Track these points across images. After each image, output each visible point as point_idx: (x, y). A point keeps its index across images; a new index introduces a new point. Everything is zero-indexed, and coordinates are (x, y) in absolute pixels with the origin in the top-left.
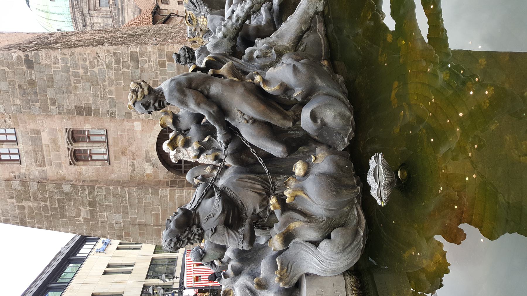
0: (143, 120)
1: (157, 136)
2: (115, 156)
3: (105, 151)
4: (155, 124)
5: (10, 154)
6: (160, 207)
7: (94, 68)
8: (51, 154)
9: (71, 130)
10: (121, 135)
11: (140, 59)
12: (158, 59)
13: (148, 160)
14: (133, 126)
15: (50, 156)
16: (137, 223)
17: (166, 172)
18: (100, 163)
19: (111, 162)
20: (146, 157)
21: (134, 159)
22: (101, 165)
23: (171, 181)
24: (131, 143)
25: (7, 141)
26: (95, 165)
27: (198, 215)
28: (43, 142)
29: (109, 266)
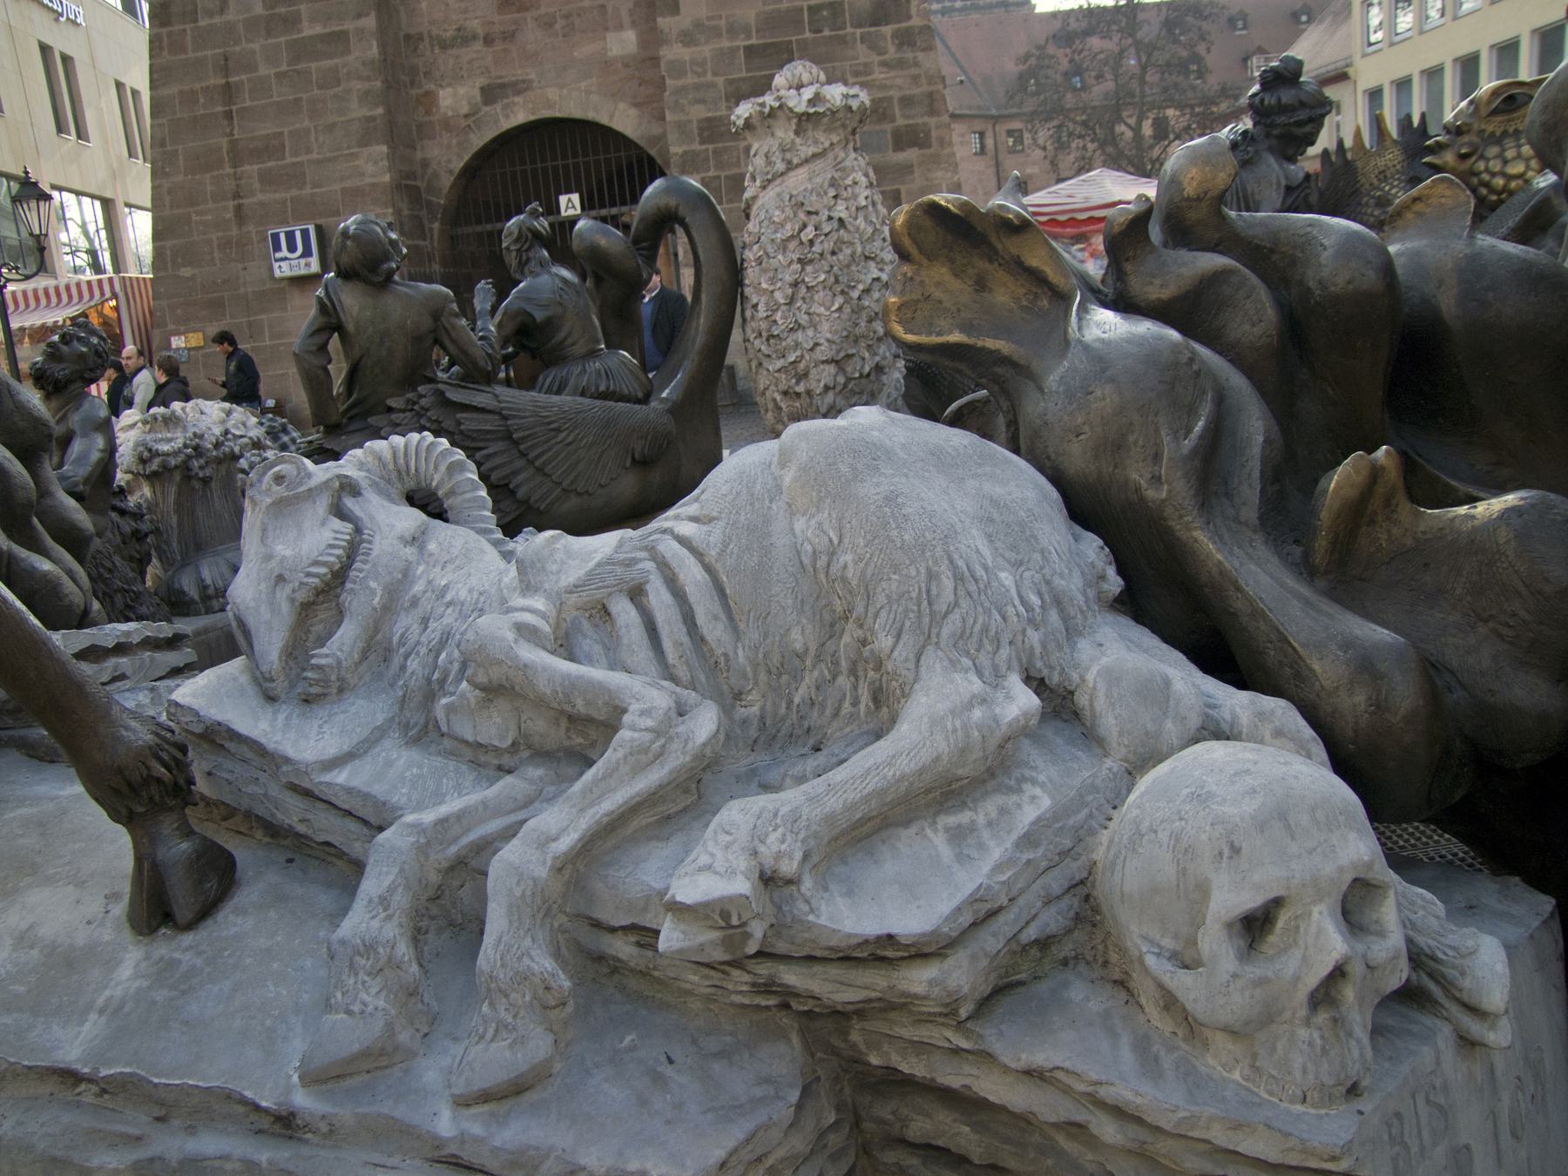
0: (655, 60)
1: (590, 115)
4: (636, 105)
6: (315, 156)
11: (887, 30)
13: (491, 94)
16: (233, 79)
17: (451, 166)
20: (503, 86)
21: (488, 40)
23: (418, 188)
24: (550, 25)
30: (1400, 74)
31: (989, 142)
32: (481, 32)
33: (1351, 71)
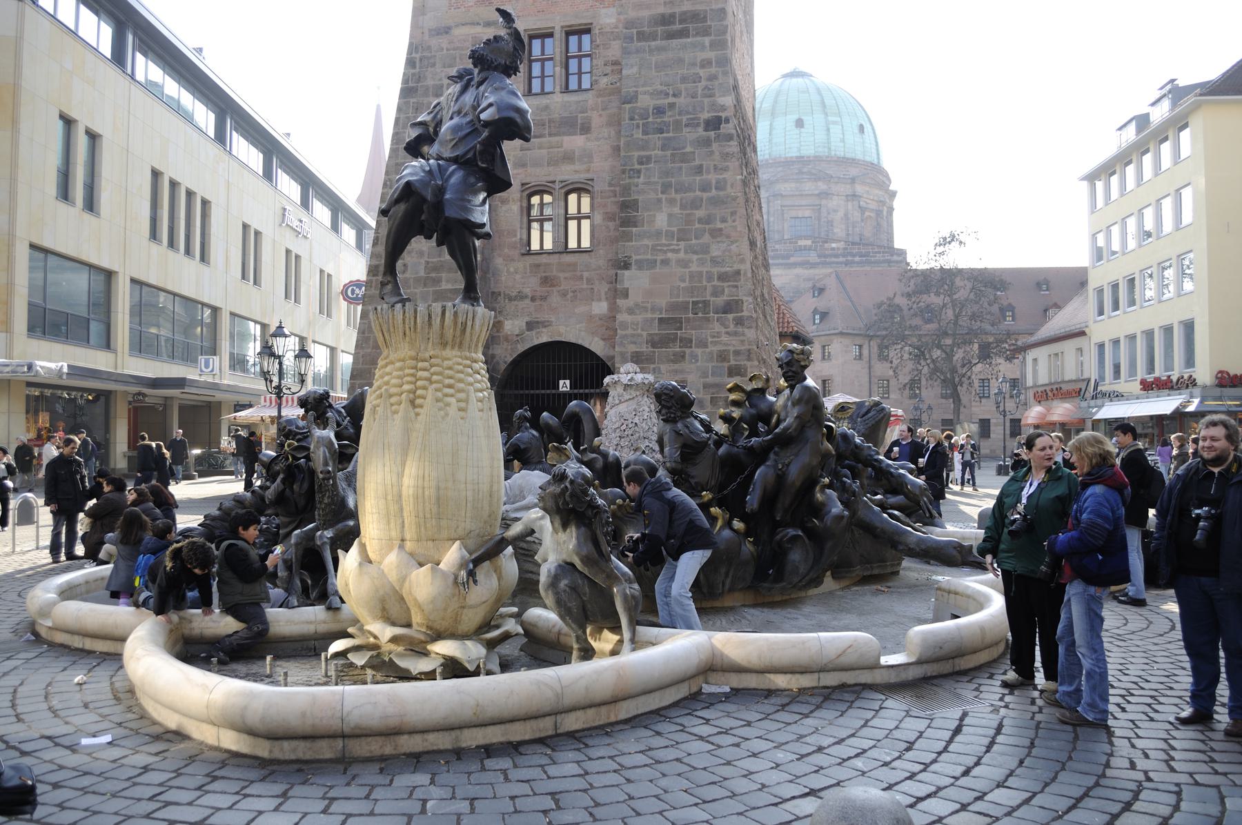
1: (580, 342)
2: (538, 266)
3: (548, 245)
4: (604, 339)
5: (543, 77)
7: (710, 234)
8: (544, 152)
9: (590, 189)
10: (581, 278)
11: (730, 316)
12: (732, 348)
13: (530, 326)
14: (600, 300)
15: (540, 148)
18: (525, 237)
19: (527, 258)
20: (538, 322)
21: (533, 299)
22: (521, 239)
25: (567, 75)
26: (521, 228)
27: (689, 417)
28: (566, 139)
29: (257, 233)
30: (1114, 336)
31: (865, 352)
32: (530, 295)
33: (1087, 331)
